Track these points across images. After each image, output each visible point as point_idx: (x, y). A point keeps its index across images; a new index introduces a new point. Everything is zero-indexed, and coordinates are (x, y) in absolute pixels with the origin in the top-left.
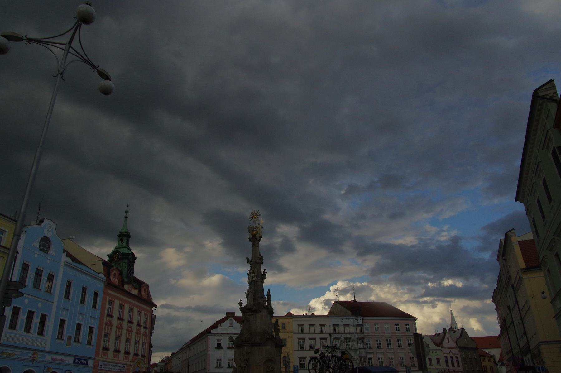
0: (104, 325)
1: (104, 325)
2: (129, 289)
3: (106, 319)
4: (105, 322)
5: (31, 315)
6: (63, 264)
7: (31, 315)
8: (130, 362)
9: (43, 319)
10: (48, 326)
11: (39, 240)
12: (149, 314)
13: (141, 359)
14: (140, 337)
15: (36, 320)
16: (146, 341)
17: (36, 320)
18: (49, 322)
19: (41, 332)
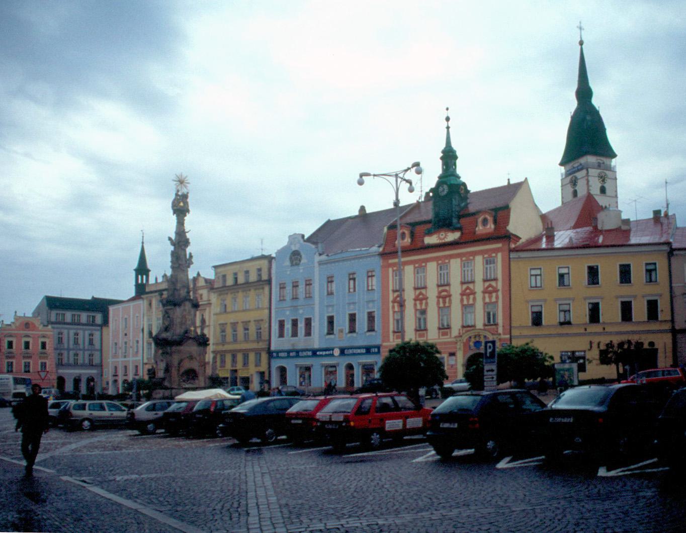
0: (391, 305)
1: (391, 305)
2: (440, 239)
3: (393, 294)
4: (391, 298)
5: (295, 323)
6: (316, 265)
7: (295, 323)
8: (456, 337)
9: (308, 322)
10: (314, 327)
11: (288, 259)
12: (499, 255)
13: (484, 330)
14: (474, 299)
15: (301, 325)
16: (497, 297)
17: (301, 325)
18: (314, 322)
19: (308, 333)
